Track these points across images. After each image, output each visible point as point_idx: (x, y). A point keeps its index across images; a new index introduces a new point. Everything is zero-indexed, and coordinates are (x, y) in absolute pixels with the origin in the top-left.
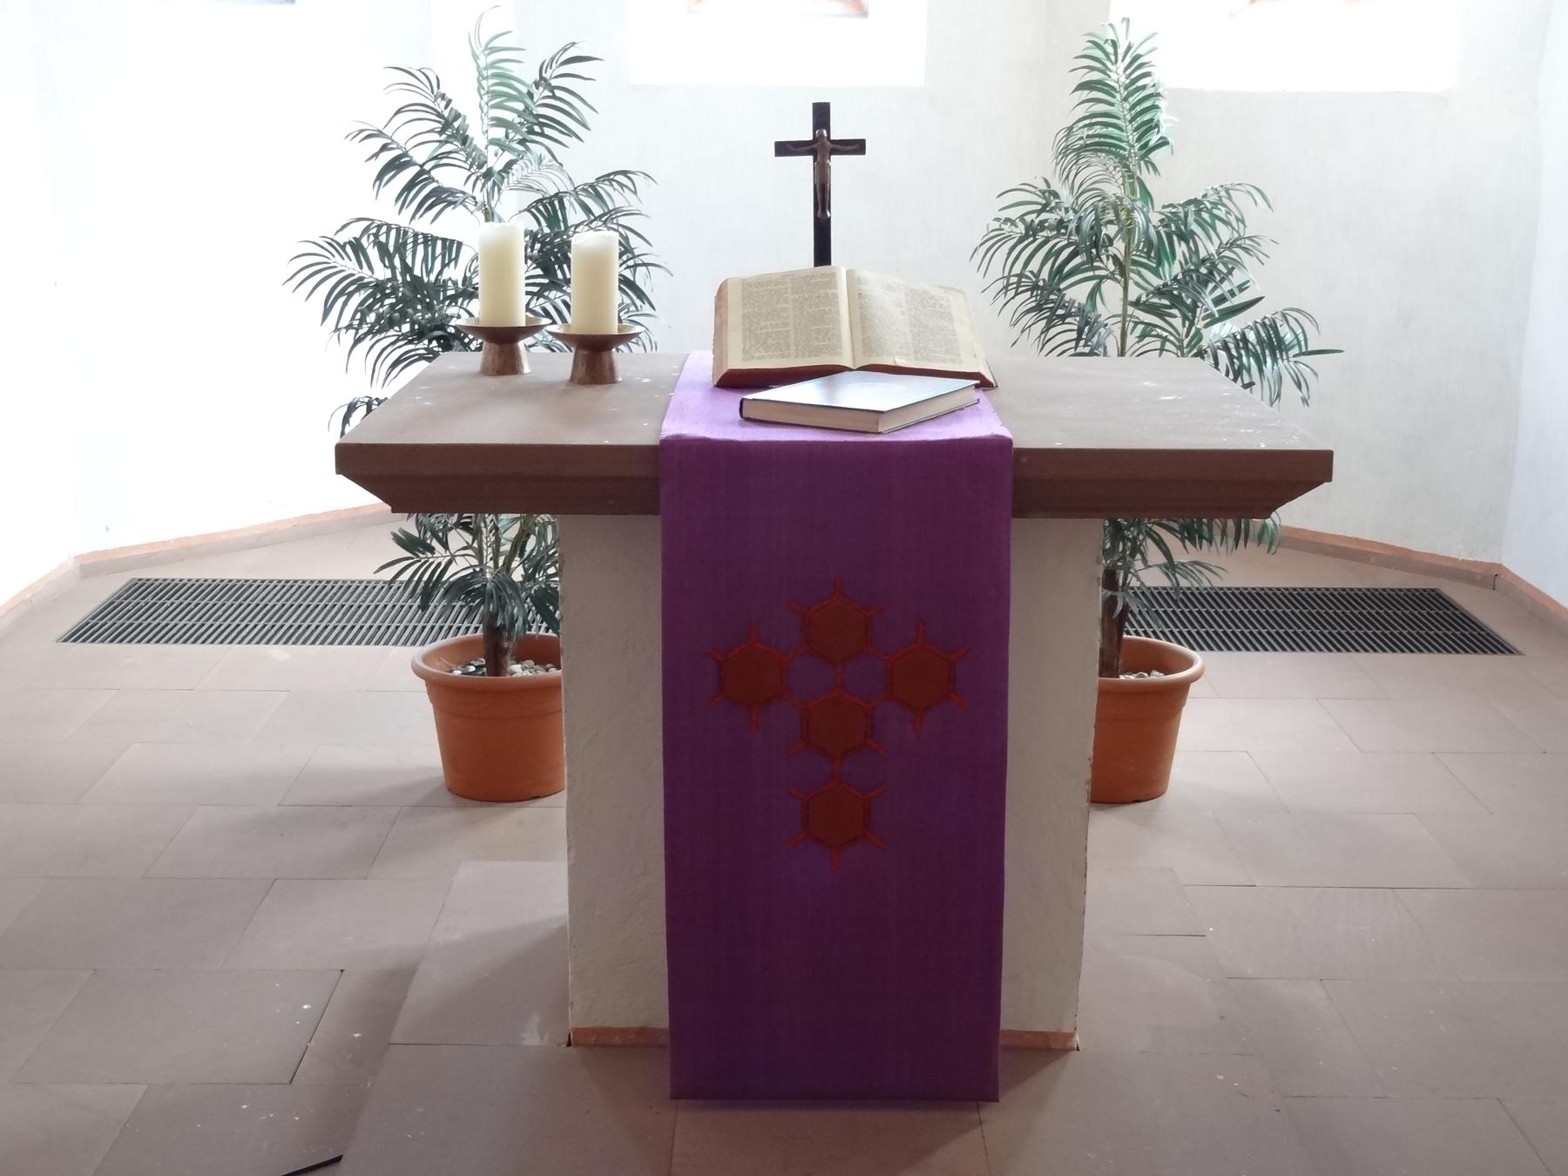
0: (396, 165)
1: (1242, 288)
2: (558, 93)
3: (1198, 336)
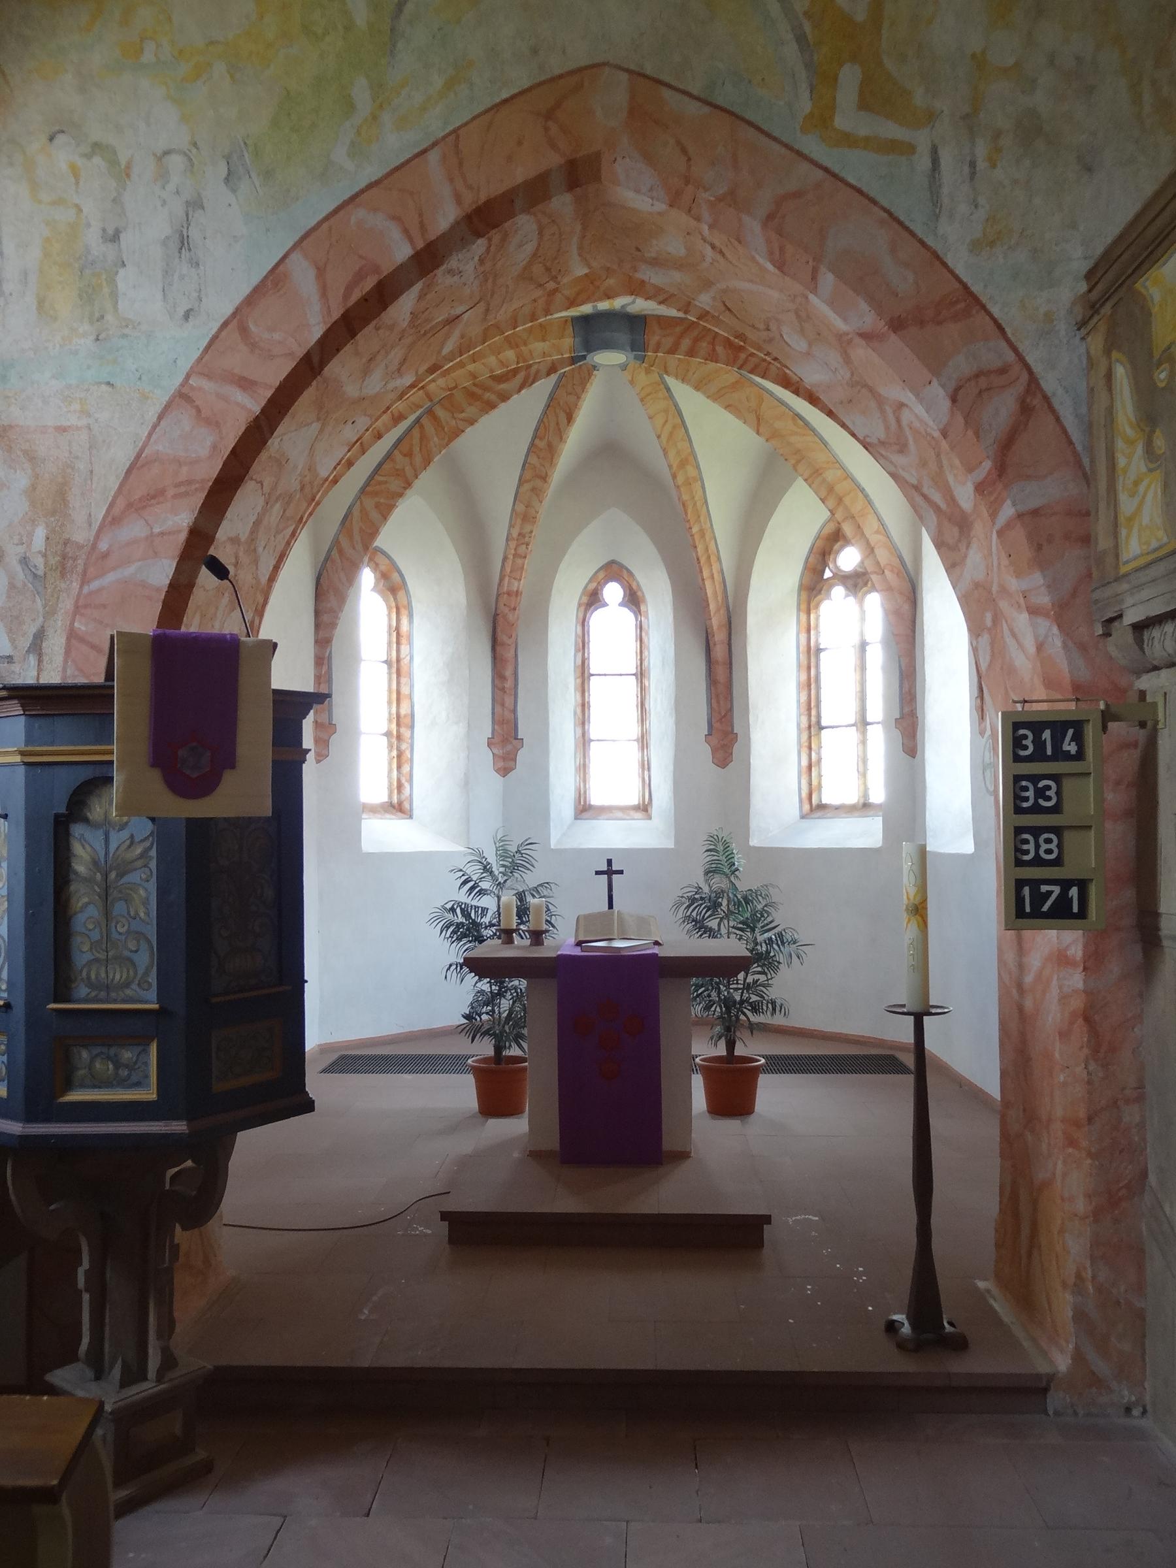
0: (465, 883)
2: (524, 855)
3: (756, 939)
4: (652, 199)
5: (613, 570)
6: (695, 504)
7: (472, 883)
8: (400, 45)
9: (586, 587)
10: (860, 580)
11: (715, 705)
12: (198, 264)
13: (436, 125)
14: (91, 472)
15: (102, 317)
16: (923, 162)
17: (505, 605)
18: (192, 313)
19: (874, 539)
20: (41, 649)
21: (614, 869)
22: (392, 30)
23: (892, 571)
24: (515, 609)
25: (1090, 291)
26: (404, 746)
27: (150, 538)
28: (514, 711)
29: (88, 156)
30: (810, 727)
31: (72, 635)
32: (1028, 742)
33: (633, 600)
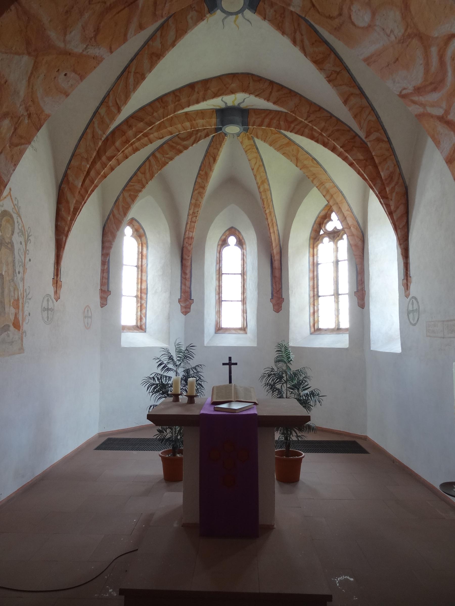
0: (160, 365)
1: (307, 385)
2: (189, 352)
3: (300, 394)
5: (232, 231)
6: (267, 201)
7: (164, 365)
9: (221, 238)
10: (336, 235)
11: (274, 286)
17: (187, 243)
19: (346, 213)
21: (232, 362)
23: (354, 227)
24: (191, 244)
26: (143, 302)
30: (314, 296)
33: (240, 243)
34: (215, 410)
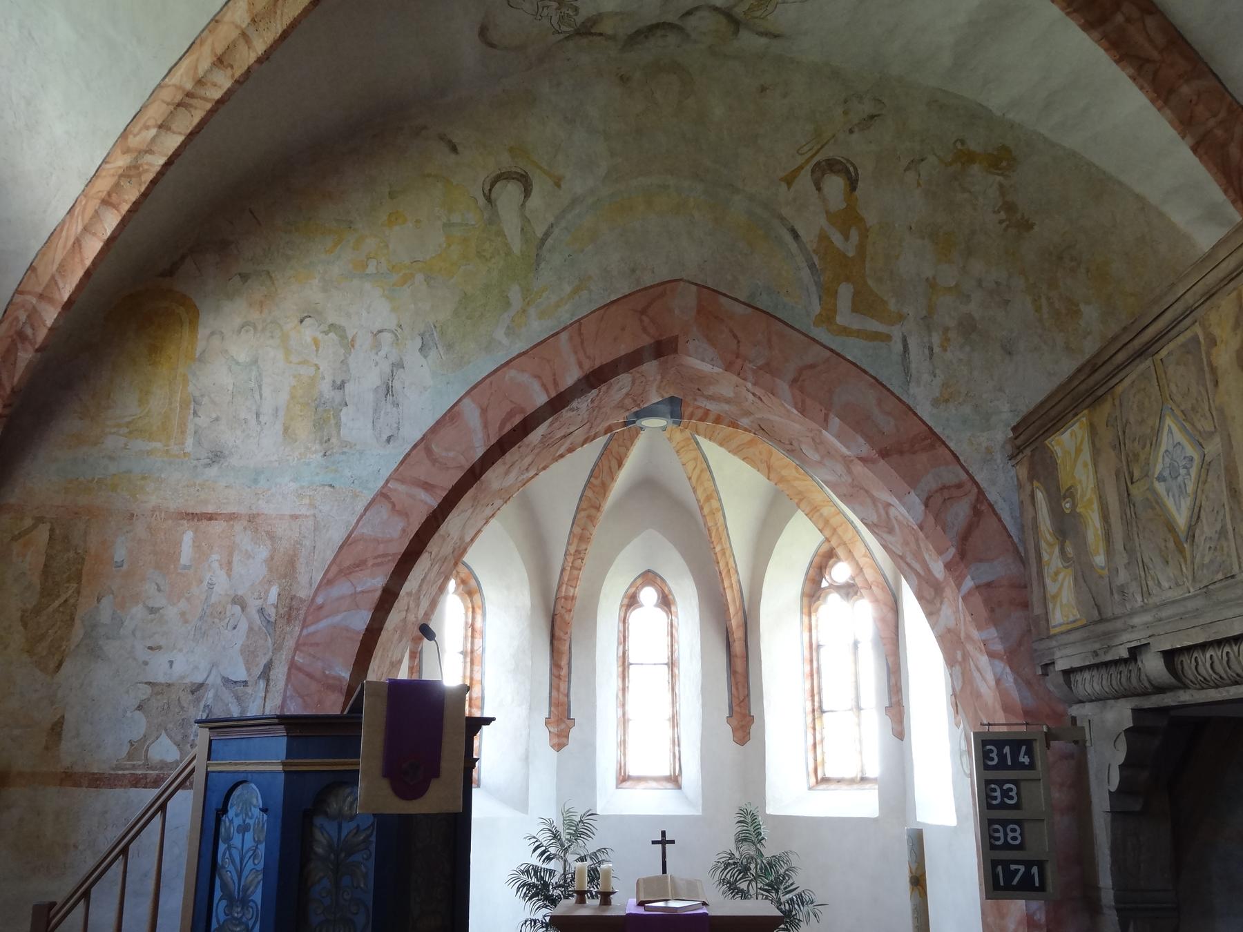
1: (792, 884)
4: (713, 366)
5: (649, 577)
6: (717, 529)
7: (544, 848)
8: (543, 265)
9: (626, 592)
10: (851, 590)
12: (398, 405)
13: (566, 315)
14: (315, 547)
15: (329, 440)
16: (898, 347)
18: (392, 438)
19: (863, 561)
20: (269, 676)
21: (667, 839)
22: (537, 255)
23: (878, 586)
24: (570, 611)
25: (1016, 438)
27: (355, 594)
28: (568, 695)
29: (326, 333)
30: (813, 711)
31: (293, 666)
32: (994, 755)
33: (666, 602)
34: (645, 911)
